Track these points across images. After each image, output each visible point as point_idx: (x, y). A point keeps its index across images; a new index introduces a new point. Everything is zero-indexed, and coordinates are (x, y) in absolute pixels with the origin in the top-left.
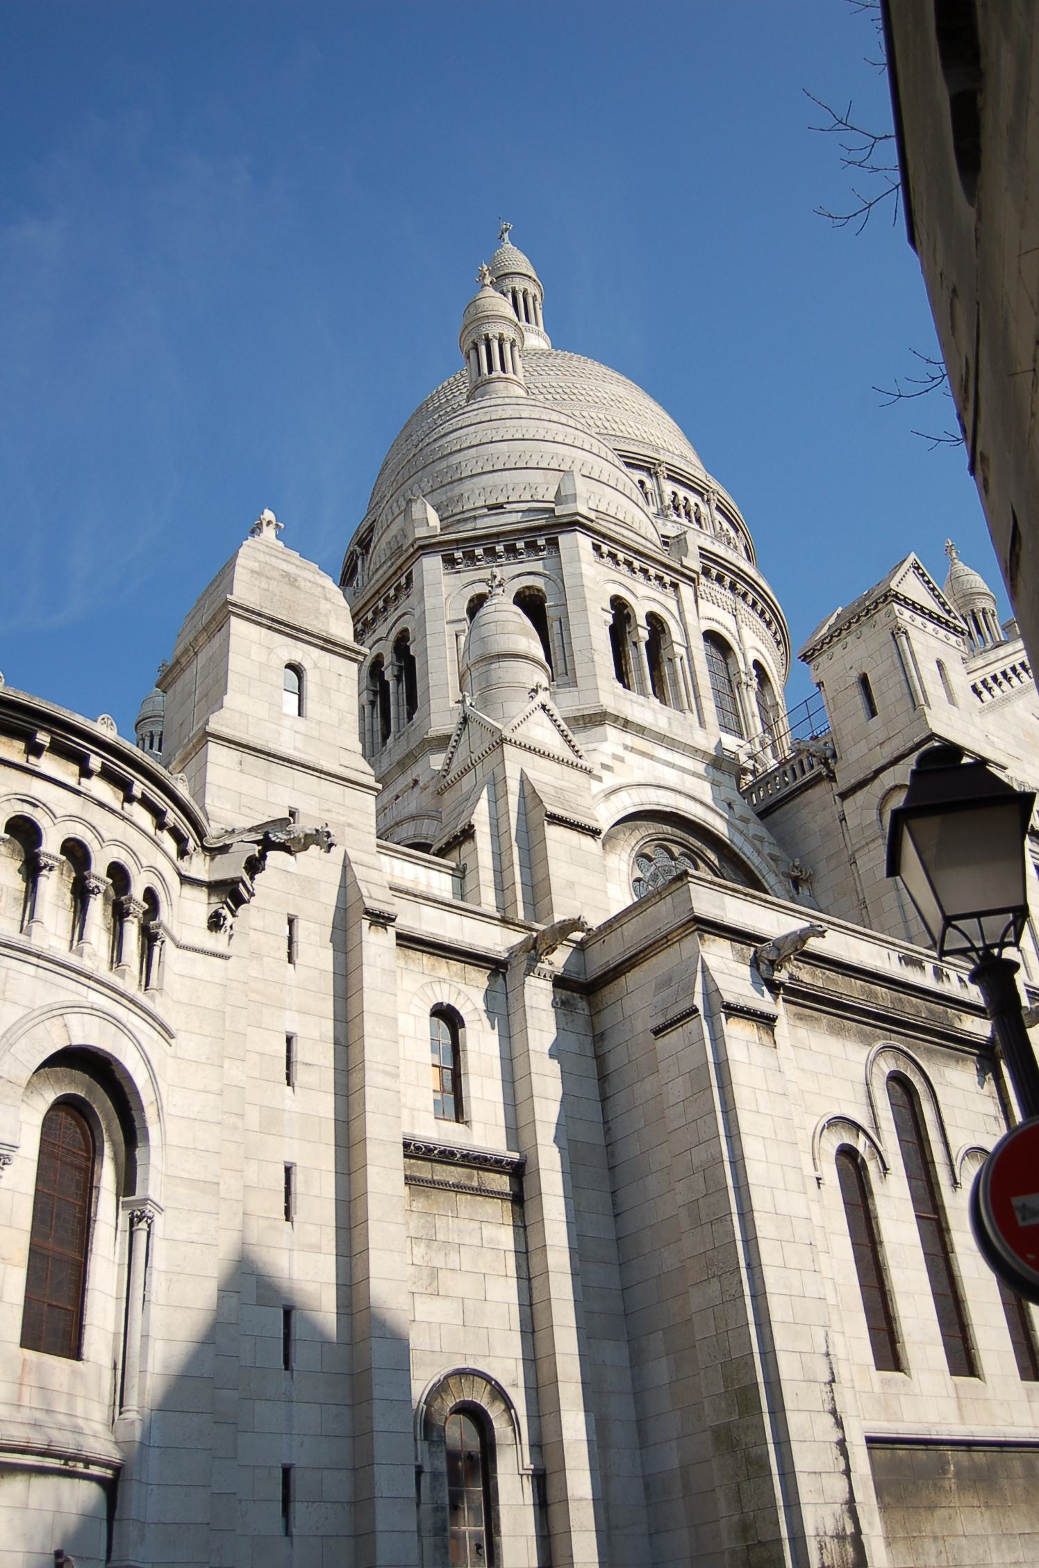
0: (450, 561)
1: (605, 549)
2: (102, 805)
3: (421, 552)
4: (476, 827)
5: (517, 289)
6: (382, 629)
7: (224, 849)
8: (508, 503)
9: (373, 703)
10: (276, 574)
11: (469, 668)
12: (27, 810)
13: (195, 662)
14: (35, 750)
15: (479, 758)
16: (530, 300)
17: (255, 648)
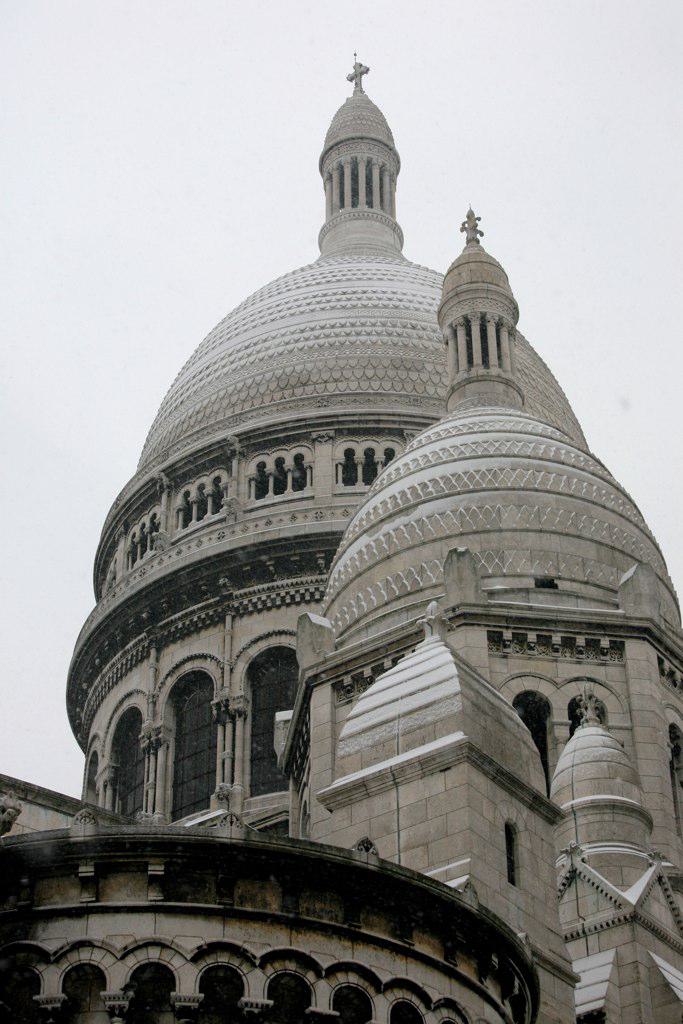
0: (495, 639)
1: (667, 664)
3: (463, 621)
4: (607, 1016)
5: (374, 161)
8: (560, 578)
10: (486, 708)
11: (574, 812)
13: (393, 793)
14: (482, 973)
15: (596, 928)
16: (386, 179)
17: (485, 801)
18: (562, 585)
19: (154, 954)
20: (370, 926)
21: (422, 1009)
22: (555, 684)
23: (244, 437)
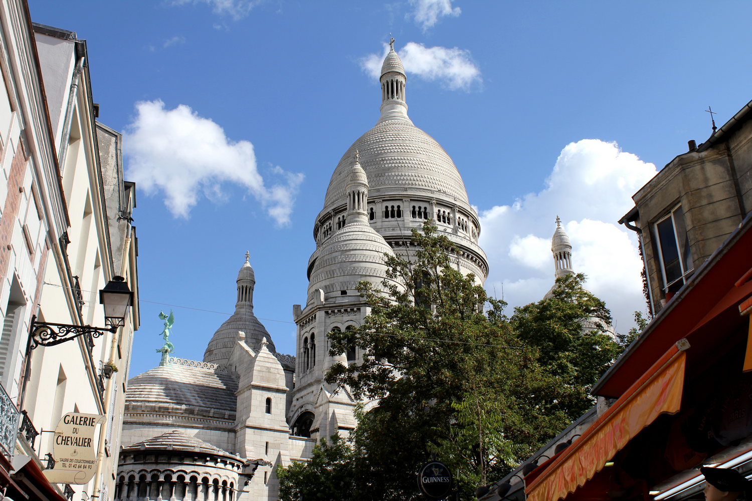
0: (327, 313)
2: (221, 468)
6: (308, 329)
7: (248, 465)
9: (305, 352)
10: (264, 370)
12: (206, 475)
18: (349, 293)
19: (132, 473)
20: (173, 460)
21: (185, 475)
22: (342, 323)
23: (334, 210)
